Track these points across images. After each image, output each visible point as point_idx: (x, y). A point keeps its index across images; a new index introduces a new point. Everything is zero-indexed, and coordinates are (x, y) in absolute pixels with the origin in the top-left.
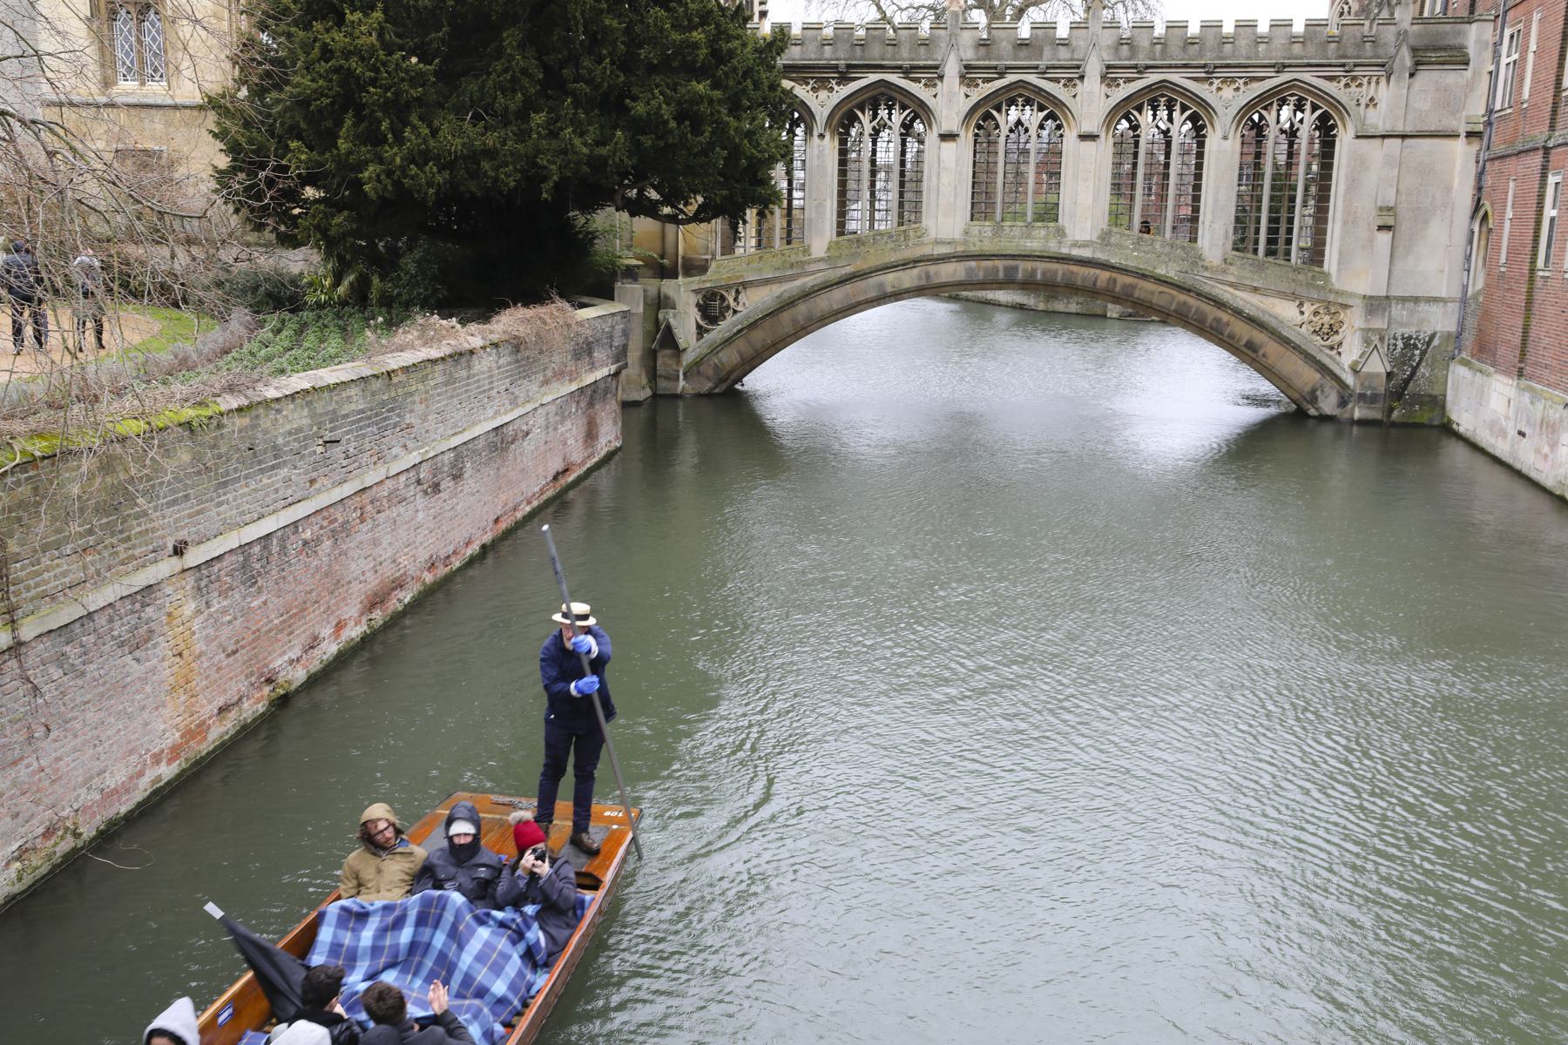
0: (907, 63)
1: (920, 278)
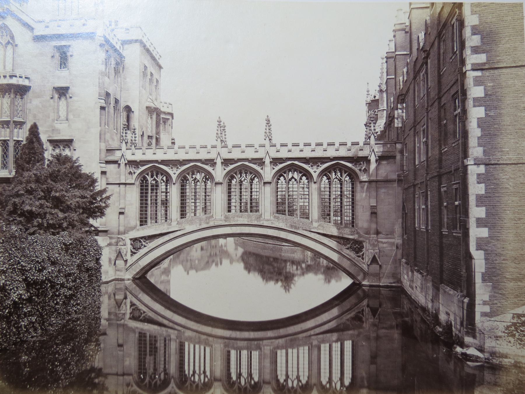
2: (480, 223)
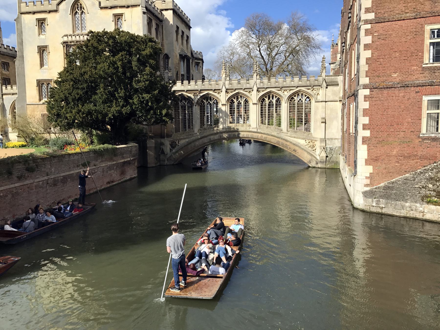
0: (213, 89)
2: (365, 127)
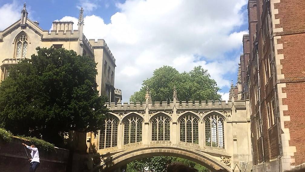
0: (138, 110)
1: (141, 153)
2: (285, 113)
